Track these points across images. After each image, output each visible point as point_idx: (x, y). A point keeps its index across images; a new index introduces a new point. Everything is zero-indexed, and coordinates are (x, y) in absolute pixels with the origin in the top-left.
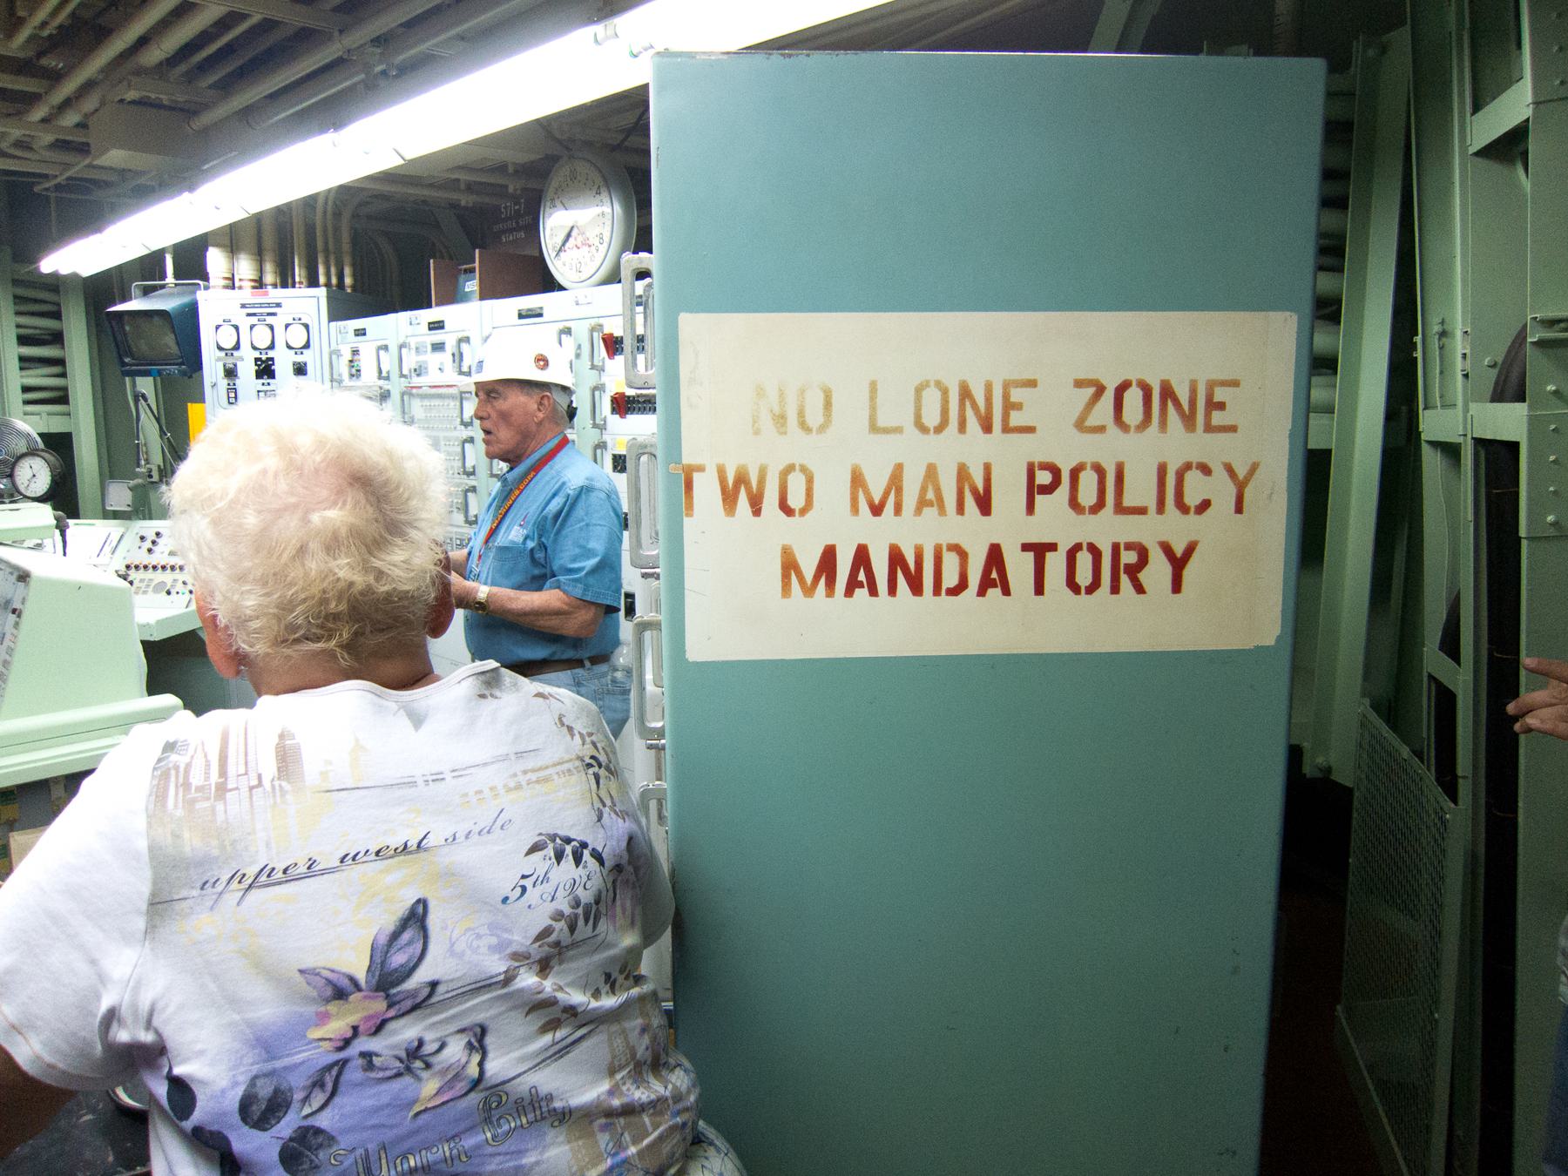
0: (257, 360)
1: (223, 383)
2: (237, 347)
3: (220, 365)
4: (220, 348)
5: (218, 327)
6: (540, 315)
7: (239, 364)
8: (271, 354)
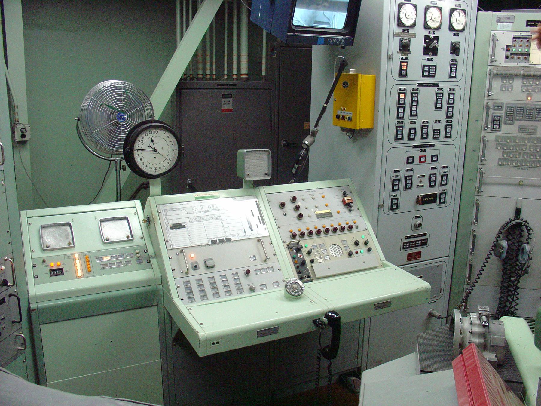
0: (427, 37)
1: (397, 57)
2: (413, 26)
3: (397, 39)
4: (400, 24)
5: (400, 6)
7: (412, 39)
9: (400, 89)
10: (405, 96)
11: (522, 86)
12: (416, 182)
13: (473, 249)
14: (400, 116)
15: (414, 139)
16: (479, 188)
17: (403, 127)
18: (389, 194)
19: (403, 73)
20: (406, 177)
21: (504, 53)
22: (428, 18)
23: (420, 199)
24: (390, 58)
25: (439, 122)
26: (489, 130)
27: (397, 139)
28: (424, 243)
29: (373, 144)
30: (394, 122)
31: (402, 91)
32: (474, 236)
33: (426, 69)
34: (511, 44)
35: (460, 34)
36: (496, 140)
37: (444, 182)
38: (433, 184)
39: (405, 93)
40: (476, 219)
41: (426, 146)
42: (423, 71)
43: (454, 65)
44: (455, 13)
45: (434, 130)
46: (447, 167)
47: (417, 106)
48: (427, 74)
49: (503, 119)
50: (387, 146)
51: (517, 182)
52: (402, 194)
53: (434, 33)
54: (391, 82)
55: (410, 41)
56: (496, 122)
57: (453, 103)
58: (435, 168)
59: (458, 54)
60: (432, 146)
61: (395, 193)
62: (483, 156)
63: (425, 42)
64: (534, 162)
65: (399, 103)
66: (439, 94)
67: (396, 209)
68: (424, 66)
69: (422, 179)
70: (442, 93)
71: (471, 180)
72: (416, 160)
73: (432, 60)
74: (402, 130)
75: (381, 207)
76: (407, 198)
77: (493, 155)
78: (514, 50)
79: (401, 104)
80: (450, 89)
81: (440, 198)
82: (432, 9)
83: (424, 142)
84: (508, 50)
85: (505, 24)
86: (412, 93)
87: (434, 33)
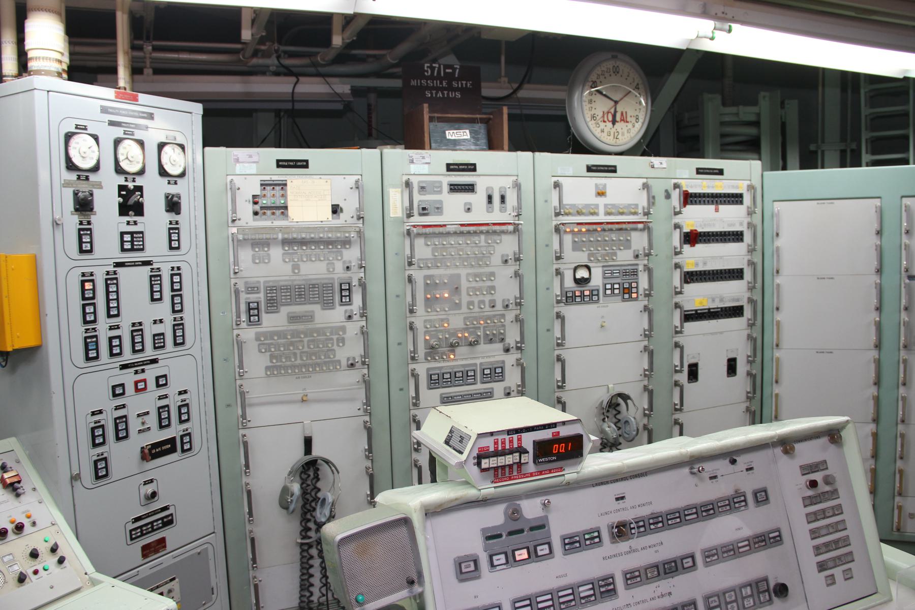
0: (121, 188)
1: (72, 222)
2: (96, 169)
3: (69, 194)
4: (71, 166)
5: (69, 137)
6: (615, 171)
7: (96, 192)
8: (139, 182)
9: (83, 275)
10: (94, 285)
11: (284, 254)
12: (135, 425)
13: (250, 513)
14: (88, 319)
15: (120, 354)
16: (244, 416)
17: (96, 336)
18: (89, 455)
19: (86, 247)
20: (116, 419)
21: (250, 208)
22: (121, 157)
23: (146, 451)
24: (56, 224)
25: (161, 321)
26: (244, 325)
27: (88, 359)
28: (168, 522)
29: (43, 375)
30: (78, 331)
31: (87, 278)
32: (249, 493)
33: (127, 238)
34: (258, 193)
35: (179, 181)
36: (257, 339)
37: (184, 417)
38: (165, 423)
39: (93, 281)
40: (247, 466)
41: (144, 363)
42: (122, 242)
43: (174, 230)
44: (167, 149)
45: (155, 335)
46: (185, 392)
47: (117, 299)
48: (129, 247)
49: (263, 307)
50: (71, 373)
51: (299, 397)
52: (113, 449)
53: (134, 181)
54: (64, 264)
55: (92, 195)
56: (253, 312)
57: (180, 290)
58: (166, 396)
59: (178, 213)
60: (154, 361)
61: (99, 450)
62: (241, 366)
63: (120, 195)
64: (318, 364)
65: (84, 298)
66: (155, 277)
67: (106, 475)
68: (122, 234)
69: (146, 418)
70: (160, 276)
71: (229, 406)
72: (130, 389)
73: (135, 223)
74: (97, 342)
75: (75, 478)
76: (123, 456)
77: (256, 362)
78: (264, 202)
79: (87, 299)
80: (173, 268)
81: (182, 444)
82: (127, 142)
83: (139, 357)
84: (255, 203)
85: (246, 165)
86: (107, 280)
87: (134, 181)
